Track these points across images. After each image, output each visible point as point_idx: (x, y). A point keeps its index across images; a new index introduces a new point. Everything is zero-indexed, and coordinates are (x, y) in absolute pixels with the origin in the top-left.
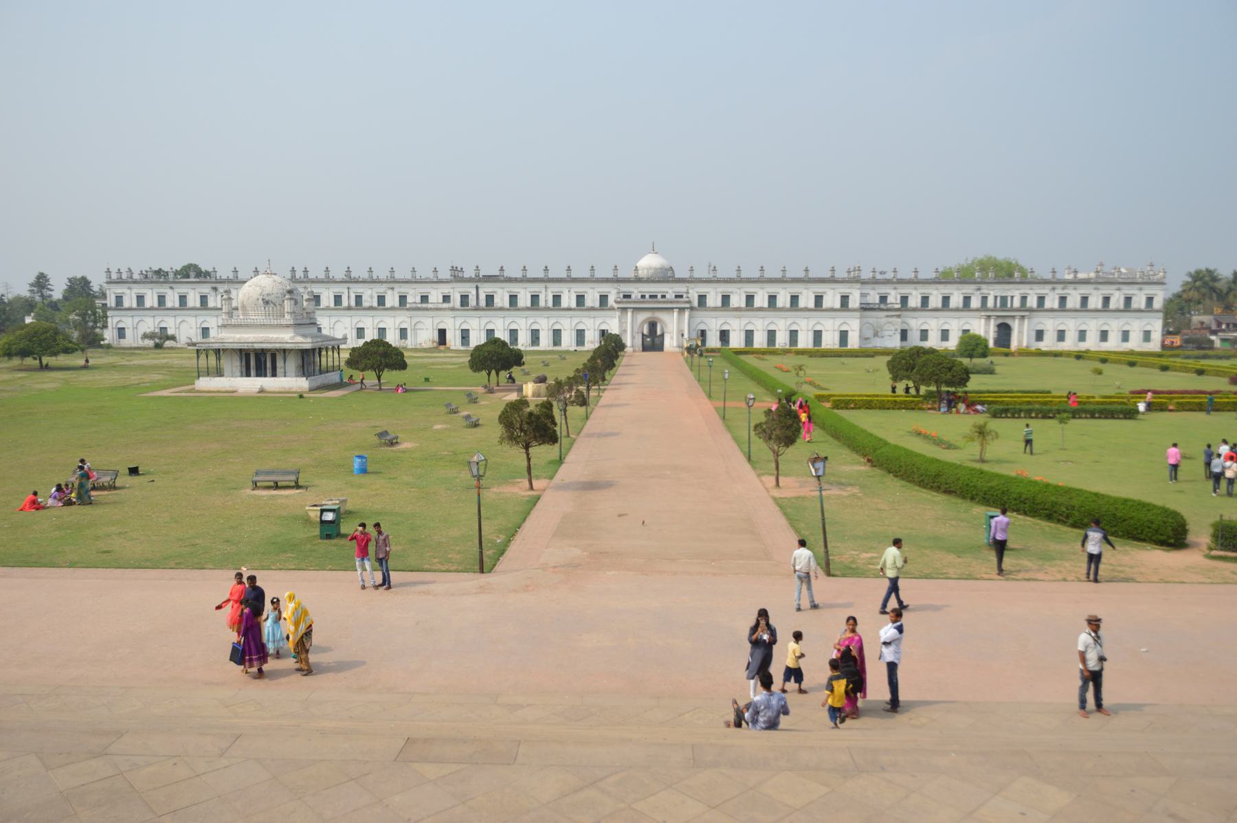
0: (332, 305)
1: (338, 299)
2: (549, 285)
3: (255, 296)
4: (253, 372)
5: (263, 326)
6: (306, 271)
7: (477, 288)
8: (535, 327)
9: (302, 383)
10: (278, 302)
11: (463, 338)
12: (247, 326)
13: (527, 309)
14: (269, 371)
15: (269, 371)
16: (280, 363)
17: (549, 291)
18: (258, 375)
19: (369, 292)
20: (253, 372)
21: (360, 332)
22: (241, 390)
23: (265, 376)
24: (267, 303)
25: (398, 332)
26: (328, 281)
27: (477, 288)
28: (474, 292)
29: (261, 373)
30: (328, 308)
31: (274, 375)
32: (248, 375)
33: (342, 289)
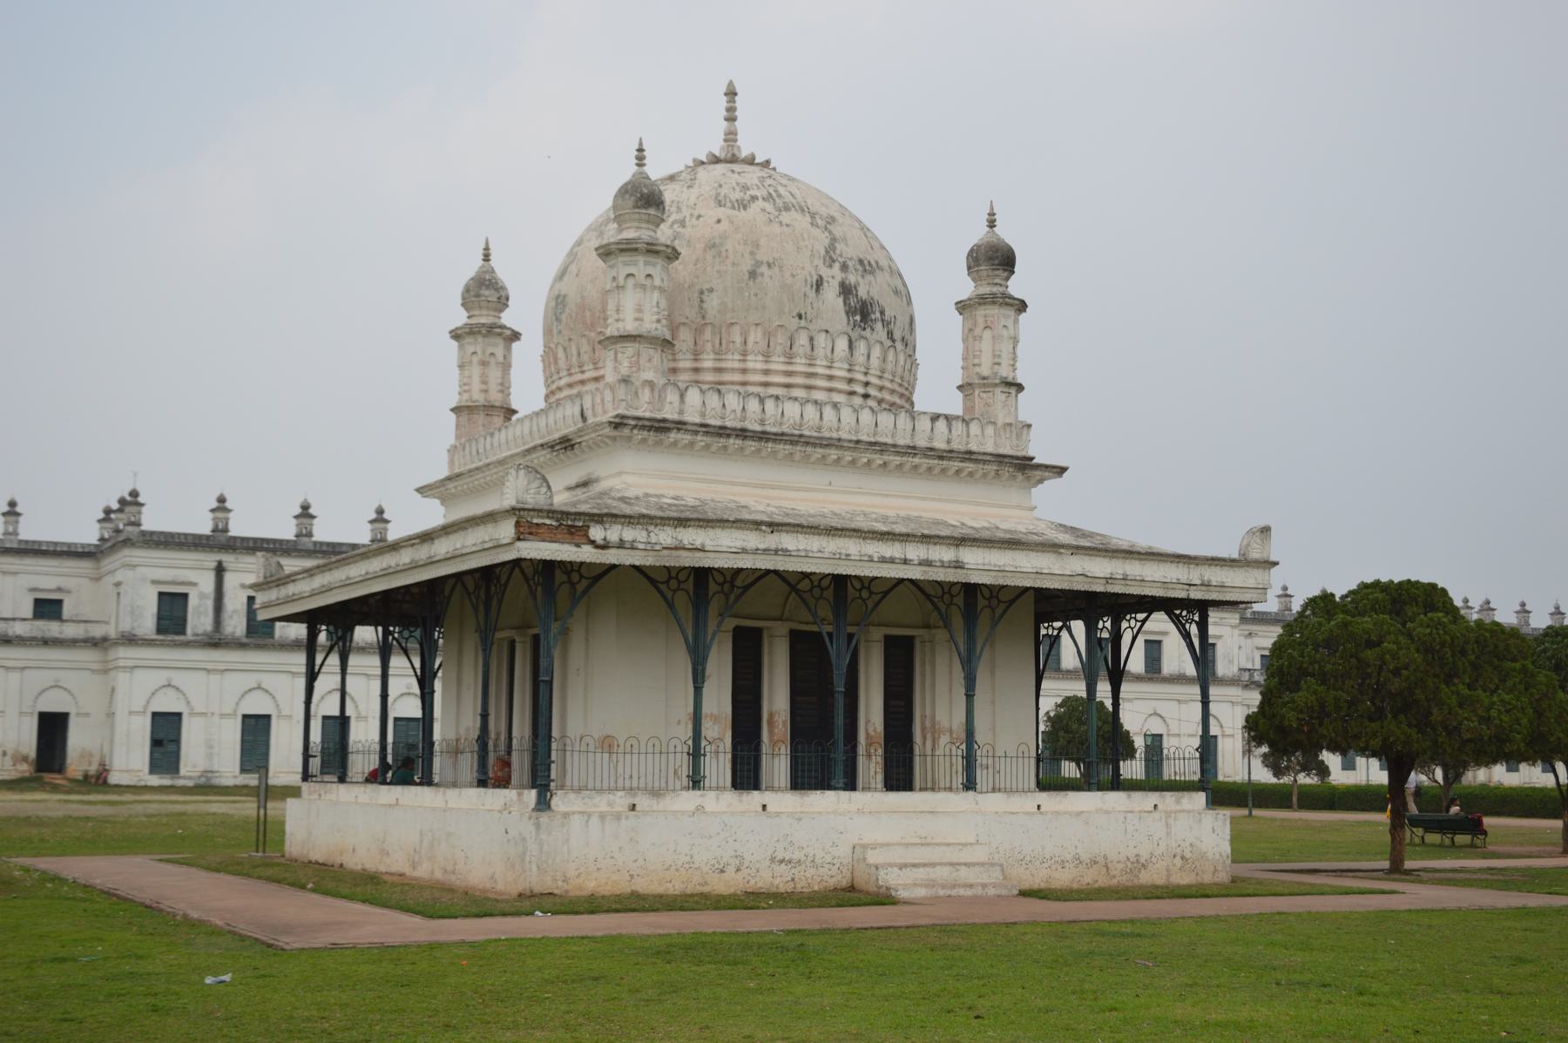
4: (777, 765)
7: (220, 570)
11: (156, 743)
14: (871, 766)
15: (871, 766)
18: (803, 780)
20: (777, 765)
27: (220, 570)
28: (207, 583)
29: (822, 763)
31: (899, 777)
32: (746, 776)
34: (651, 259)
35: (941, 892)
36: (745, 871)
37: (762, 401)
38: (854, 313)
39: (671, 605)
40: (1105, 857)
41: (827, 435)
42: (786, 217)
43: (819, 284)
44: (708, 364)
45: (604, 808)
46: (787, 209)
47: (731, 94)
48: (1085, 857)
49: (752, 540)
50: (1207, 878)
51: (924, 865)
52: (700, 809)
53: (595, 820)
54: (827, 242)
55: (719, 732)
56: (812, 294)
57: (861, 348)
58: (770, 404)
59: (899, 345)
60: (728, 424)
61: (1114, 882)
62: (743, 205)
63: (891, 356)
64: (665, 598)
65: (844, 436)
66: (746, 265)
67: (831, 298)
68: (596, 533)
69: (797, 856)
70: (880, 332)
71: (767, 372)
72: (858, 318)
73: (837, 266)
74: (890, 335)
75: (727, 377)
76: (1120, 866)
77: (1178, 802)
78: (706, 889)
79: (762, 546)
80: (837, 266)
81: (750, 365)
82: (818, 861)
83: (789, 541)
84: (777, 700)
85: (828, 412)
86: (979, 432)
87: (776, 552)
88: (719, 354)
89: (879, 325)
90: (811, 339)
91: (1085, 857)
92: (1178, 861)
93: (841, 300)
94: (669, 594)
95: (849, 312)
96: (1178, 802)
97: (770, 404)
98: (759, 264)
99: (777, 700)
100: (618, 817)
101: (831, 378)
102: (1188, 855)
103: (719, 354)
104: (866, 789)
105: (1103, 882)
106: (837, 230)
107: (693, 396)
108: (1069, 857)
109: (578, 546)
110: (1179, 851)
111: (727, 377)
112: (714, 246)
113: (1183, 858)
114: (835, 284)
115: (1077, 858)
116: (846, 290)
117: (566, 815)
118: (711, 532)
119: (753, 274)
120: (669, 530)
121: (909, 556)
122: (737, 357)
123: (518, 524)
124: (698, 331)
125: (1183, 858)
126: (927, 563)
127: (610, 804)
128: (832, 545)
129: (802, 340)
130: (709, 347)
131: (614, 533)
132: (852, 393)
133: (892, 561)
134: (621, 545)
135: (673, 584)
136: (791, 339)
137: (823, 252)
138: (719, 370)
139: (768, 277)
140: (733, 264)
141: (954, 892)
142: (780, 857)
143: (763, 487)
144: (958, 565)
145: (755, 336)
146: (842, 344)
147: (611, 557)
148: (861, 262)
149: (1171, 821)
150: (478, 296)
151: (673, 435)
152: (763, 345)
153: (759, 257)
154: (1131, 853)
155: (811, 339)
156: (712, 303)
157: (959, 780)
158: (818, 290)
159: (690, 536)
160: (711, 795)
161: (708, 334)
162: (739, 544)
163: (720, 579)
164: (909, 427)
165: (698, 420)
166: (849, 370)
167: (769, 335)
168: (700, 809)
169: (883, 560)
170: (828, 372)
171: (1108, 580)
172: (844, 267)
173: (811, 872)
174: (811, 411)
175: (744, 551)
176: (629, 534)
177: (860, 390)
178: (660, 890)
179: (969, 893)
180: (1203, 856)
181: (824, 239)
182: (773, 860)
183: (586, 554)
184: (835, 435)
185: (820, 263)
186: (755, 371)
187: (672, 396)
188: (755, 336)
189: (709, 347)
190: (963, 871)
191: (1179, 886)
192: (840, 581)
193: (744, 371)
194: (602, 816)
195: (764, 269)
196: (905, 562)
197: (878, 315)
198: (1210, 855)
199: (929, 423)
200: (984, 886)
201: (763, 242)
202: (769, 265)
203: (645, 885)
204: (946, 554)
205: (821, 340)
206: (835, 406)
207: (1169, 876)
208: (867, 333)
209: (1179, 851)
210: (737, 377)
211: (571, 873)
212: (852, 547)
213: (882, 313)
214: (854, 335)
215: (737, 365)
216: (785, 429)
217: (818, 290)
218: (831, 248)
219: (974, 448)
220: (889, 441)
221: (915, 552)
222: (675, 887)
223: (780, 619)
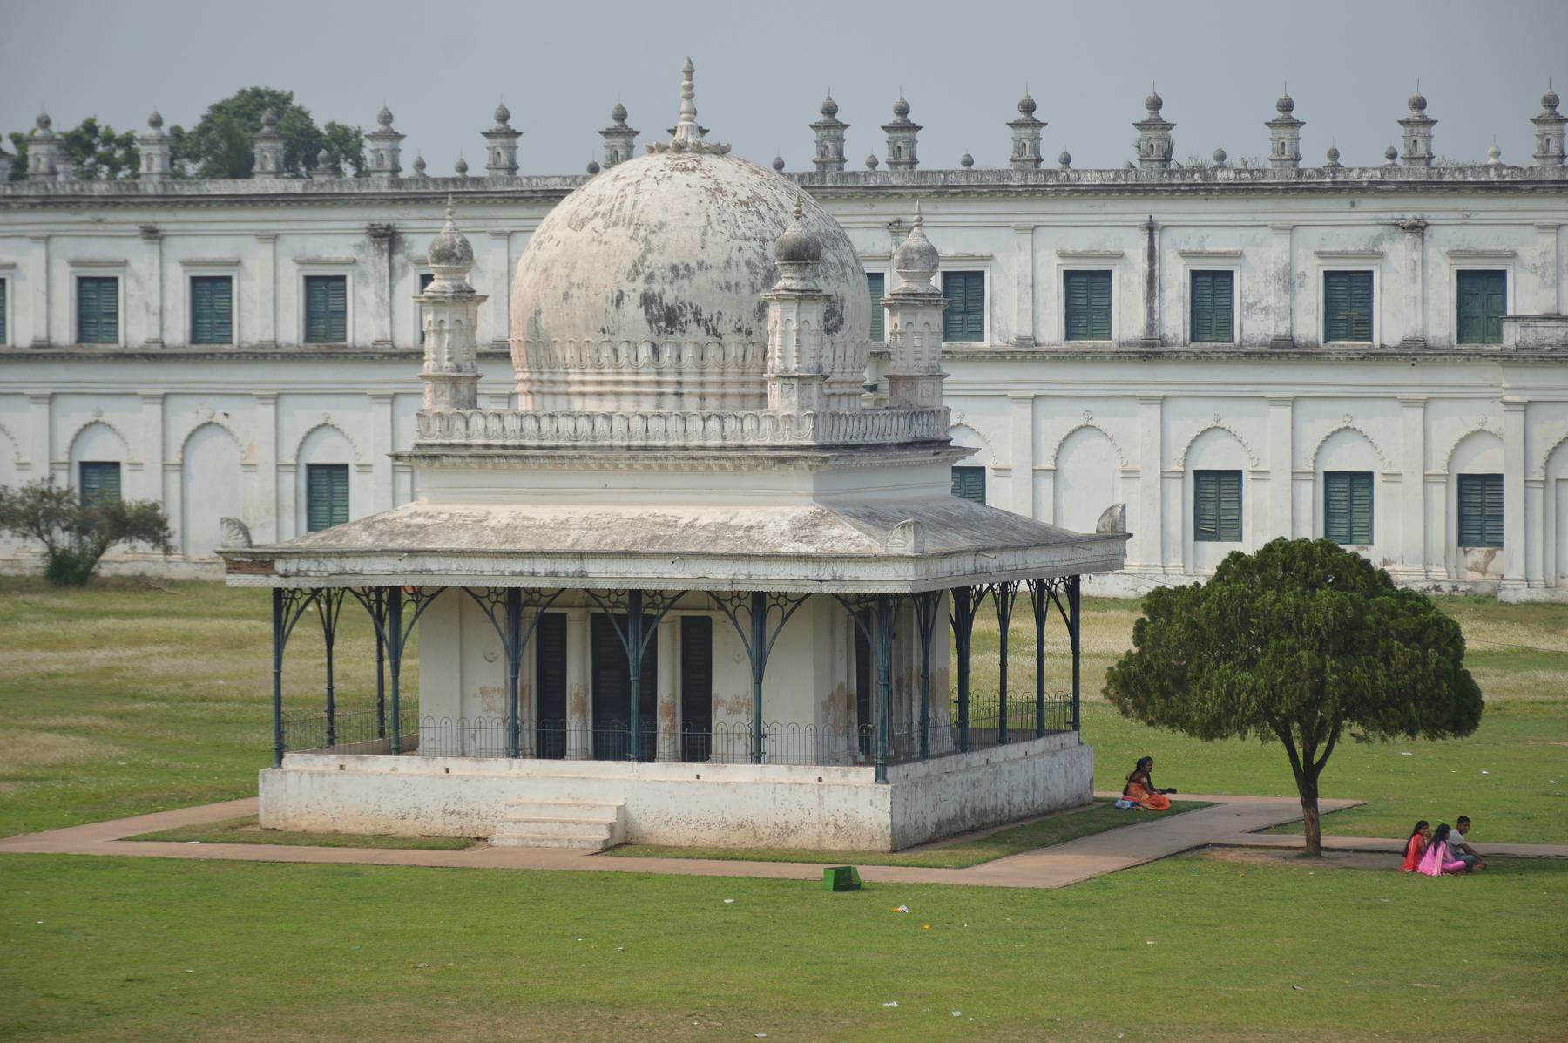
0: (1052, 330)
1: (1086, 294)
3: (605, 281)
4: (577, 729)
5: (645, 455)
6: (903, 126)
9: (852, 803)
10: (733, 311)
12: (553, 455)
16: (729, 680)
19: (1275, 250)
20: (577, 729)
21: (1216, 497)
22: (507, 836)
24: (668, 318)
25: (1444, 500)
26: (1034, 183)
30: (1025, 352)
33: (1109, 233)
36: (422, 820)
37: (538, 419)
38: (659, 320)
40: (753, 822)
41: (599, 444)
43: (619, 300)
45: (320, 768)
46: (615, 224)
47: (689, 73)
50: (864, 846)
51: (536, 821)
53: (305, 777)
54: (638, 254)
57: (667, 353)
59: (730, 338)
61: (762, 844)
63: (713, 352)
65: (616, 443)
66: (561, 290)
67: (633, 311)
68: (280, 566)
69: (464, 809)
70: (695, 333)
71: (583, 383)
72: (663, 324)
73: (642, 277)
74: (713, 332)
76: (768, 831)
77: (844, 775)
78: (392, 831)
80: (642, 277)
81: (571, 377)
82: (483, 814)
83: (432, 564)
86: (754, 426)
87: (421, 572)
89: (694, 326)
90: (615, 350)
91: (731, 821)
93: (642, 311)
95: (652, 320)
96: (844, 775)
97: (545, 422)
101: (637, 383)
102: (841, 823)
106: (655, 240)
107: (477, 423)
113: (836, 826)
114: (637, 297)
115: (724, 822)
116: (647, 300)
118: (367, 560)
119: (566, 296)
120: (335, 561)
121: (537, 569)
125: (836, 826)
126: (554, 574)
127: (326, 765)
128: (468, 564)
129: (606, 352)
131: (293, 566)
132: (661, 394)
133: (521, 574)
134: (297, 574)
137: (629, 267)
138: (553, 382)
139: (579, 300)
141: (542, 844)
142: (451, 808)
144: (582, 574)
146: (645, 352)
148: (674, 268)
149: (824, 793)
154: (781, 819)
155: (615, 350)
156: (543, 322)
158: (618, 305)
159: (350, 564)
162: (391, 568)
164: (680, 428)
165: (481, 441)
166: (659, 374)
167: (579, 349)
168: (394, 769)
169: (513, 574)
170: (634, 378)
171: (732, 581)
172: (650, 278)
173: (476, 822)
174: (583, 425)
175: (394, 573)
176: (304, 565)
177: (669, 390)
178: (355, 830)
179: (556, 845)
180: (859, 825)
181: (636, 250)
182: (444, 811)
184: (607, 443)
185: (622, 278)
187: (459, 424)
188: (570, 352)
191: (830, 852)
194: (311, 774)
195: (574, 291)
196: (533, 574)
197: (690, 316)
198: (867, 825)
199: (700, 424)
204: (572, 566)
205: (623, 351)
207: (820, 842)
208: (677, 334)
211: (290, 814)
212: (486, 565)
213: (697, 313)
214: (658, 341)
216: (561, 443)
217: (618, 305)
218: (643, 259)
219: (750, 442)
221: (542, 566)
222: (368, 828)
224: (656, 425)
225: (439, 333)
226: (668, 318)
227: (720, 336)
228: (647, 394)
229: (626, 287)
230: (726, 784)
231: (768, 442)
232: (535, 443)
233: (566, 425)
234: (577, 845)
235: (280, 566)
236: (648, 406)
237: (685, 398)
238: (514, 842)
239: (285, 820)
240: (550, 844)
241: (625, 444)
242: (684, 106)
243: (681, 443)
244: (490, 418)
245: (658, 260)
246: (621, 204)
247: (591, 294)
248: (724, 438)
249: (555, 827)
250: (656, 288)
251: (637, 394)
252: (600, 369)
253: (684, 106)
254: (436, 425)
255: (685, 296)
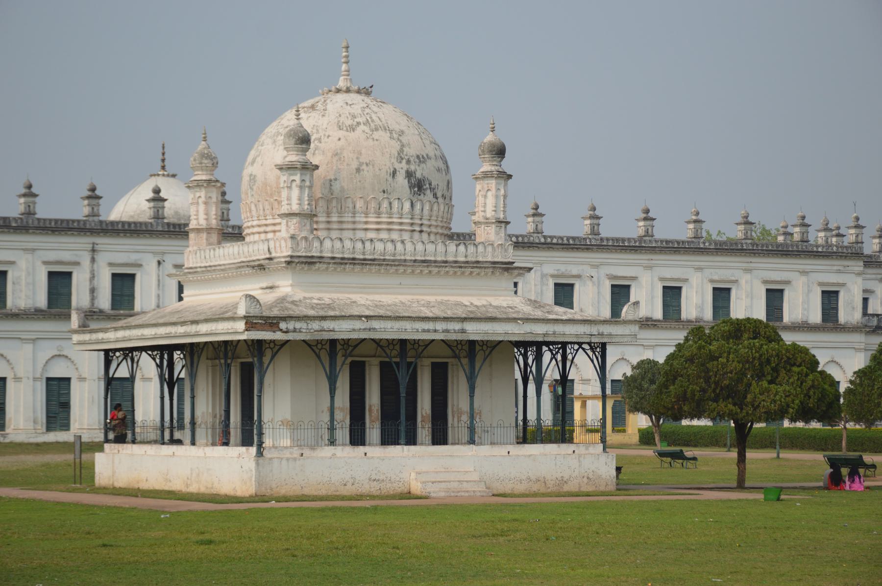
2: (102, 241)
4: (373, 432)
8: (59, 371)
12: (364, 262)
13: (35, 314)
14: (424, 431)
15: (424, 431)
17: (103, 259)
18: (388, 439)
20: (373, 432)
21: (721, 295)
23: (412, 440)
29: (398, 430)
31: (440, 437)
32: (357, 438)
34: (304, 172)
35: (452, 494)
37: (363, 242)
38: (414, 187)
39: (319, 357)
40: (544, 478)
41: (399, 258)
42: (376, 135)
43: (394, 173)
44: (335, 219)
45: (288, 456)
46: (377, 129)
48: (533, 478)
49: (358, 325)
52: (334, 455)
53: (284, 462)
54: (398, 148)
55: (343, 417)
56: (390, 179)
57: (418, 206)
58: (368, 244)
59: (440, 200)
60: (346, 256)
61: (549, 490)
62: (352, 128)
63: (435, 207)
64: (315, 352)
65: (408, 258)
66: (355, 165)
67: (401, 180)
68: (283, 325)
69: (382, 478)
70: (429, 195)
72: (416, 189)
73: (404, 161)
74: (435, 196)
75: (345, 226)
76: (553, 482)
77: (587, 449)
78: (338, 493)
79: (363, 327)
80: (404, 161)
81: (357, 219)
82: (393, 480)
83: (376, 324)
84: (373, 398)
85: (399, 246)
87: (370, 329)
88: (340, 213)
89: (428, 191)
90: (390, 203)
92: (585, 480)
93: (406, 181)
94: (317, 351)
96: (587, 449)
97: (368, 244)
98: (361, 164)
99: (373, 398)
100: (295, 459)
101: (401, 224)
102: (591, 476)
103: (340, 213)
104: (422, 444)
105: (543, 490)
106: (404, 139)
107: (328, 244)
108: (524, 478)
109: (274, 332)
110: (586, 474)
111: (345, 226)
112: (337, 154)
114: (403, 172)
115: (529, 479)
116: (409, 175)
117: (271, 459)
119: (358, 170)
120: (317, 322)
122: (350, 215)
123: (246, 323)
124: (329, 201)
127: (291, 453)
129: (385, 204)
130: (335, 210)
131: (291, 325)
132: (413, 231)
133: (428, 331)
134: (295, 330)
135: (320, 346)
136: (380, 204)
138: (341, 222)
139: (367, 172)
140: (348, 165)
141: (459, 494)
142: (373, 477)
143: (364, 288)
144: (463, 331)
145: (359, 204)
146: (407, 206)
147: (290, 337)
148: (418, 157)
149: (582, 459)
150: (201, 163)
151: (317, 265)
152: (364, 209)
153: (361, 160)
154: (559, 475)
155: (390, 203)
156: (336, 187)
157: (466, 438)
158: (393, 176)
159: (327, 325)
160: (340, 448)
161: (334, 203)
162: (351, 327)
163: (342, 343)
165: (330, 255)
166: (412, 219)
167: (367, 203)
168: (334, 455)
169: (424, 331)
170: (400, 221)
172: (408, 162)
173: (389, 485)
174: (390, 246)
175: (354, 330)
176: (298, 325)
177: (418, 228)
178: (315, 493)
179: (467, 494)
180: (600, 477)
181: (396, 146)
182: (370, 479)
183: (278, 336)
184: (403, 258)
185: (394, 160)
186: (360, 222)
189: (335, 210)
190: (465, 485)
192: (403, 342)
193: (354, 223)
194: (288, 459)
195: (364, 167)
196: (435, 331)
197: (428, 186)
198: (604, 476)
199: (455, 248)
200: (474, 491)
201: (363, 151)
202: (367, 165)
203: (306, 491)
204: (457, 326)
205: (396, 204)
206: (403, 242)
207: (580, 487)
209: (586, 474)
210: (350, 226)
211: (274, 486)
212: (408, 325)
213: (430, 184)
215: (350, 219)
217: (393, 176)
218: (401, 151)
219: (480, 259)
220: (432, 259)
221: (440, 326)
222: (323, 492)
223: (374, 356)
224: (430, 247)
225: (301, 188)
226: (418, 186)
227: (437, 198)
228: (406, 230)
229: (397, 166)
230: (530, 456)
231: (490, 259)
232: (362, 257)
233: (380, 246)
234: (479, 494)
235: (283, 325)
236: (406, 236)
237: (423, 234)
238: (442, 494)
239: (271, 489)
240: (463, 494)
241: (413, 258)
242: (344, 67)
243: (444, 259)
244: (335, 241)
245: (411, 152)
246: (371, 118)
247: (377, 170)
248: (466, 257)
249: (456, 485)
250: (412, 168)
251: (401, 230)
252: (378, 214)
253: (344, 67)
254: (303, 244)
255: (426, 174)
